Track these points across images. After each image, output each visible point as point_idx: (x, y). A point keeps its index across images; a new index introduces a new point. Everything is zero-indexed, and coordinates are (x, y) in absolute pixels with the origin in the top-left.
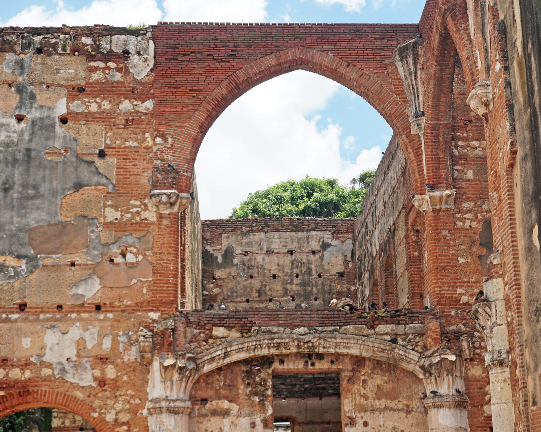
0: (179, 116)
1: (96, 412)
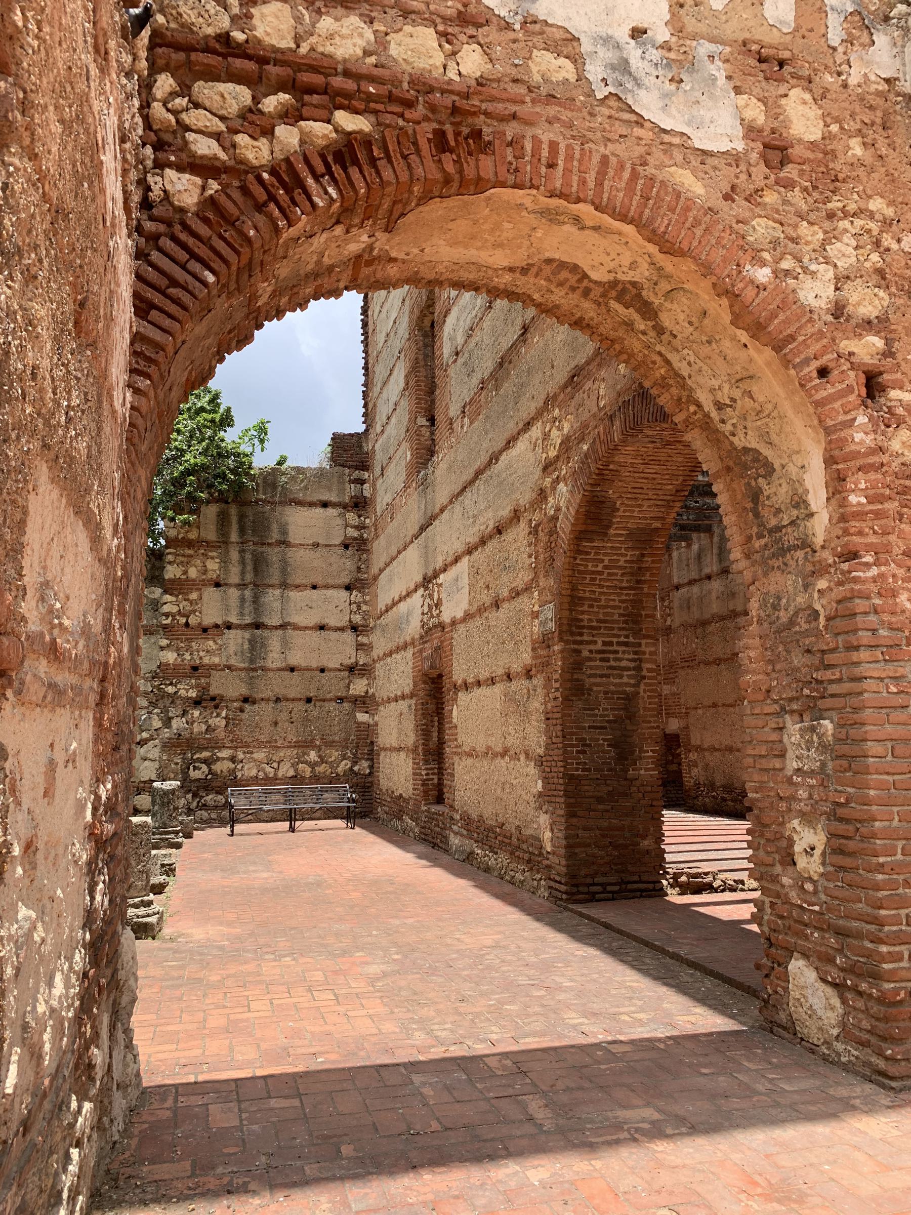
1: (763, 264)
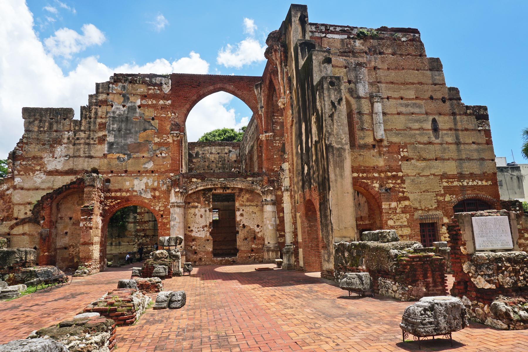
0: (180, 106)
